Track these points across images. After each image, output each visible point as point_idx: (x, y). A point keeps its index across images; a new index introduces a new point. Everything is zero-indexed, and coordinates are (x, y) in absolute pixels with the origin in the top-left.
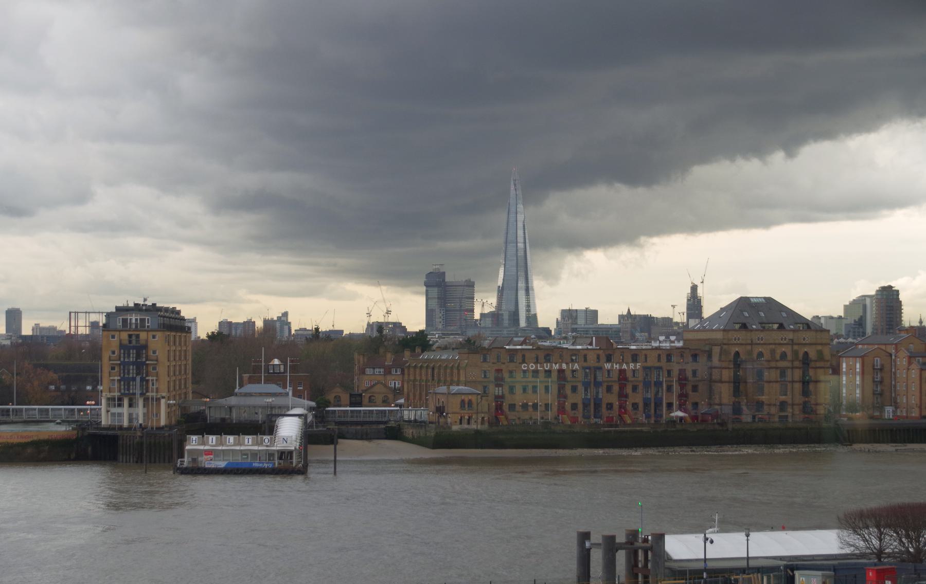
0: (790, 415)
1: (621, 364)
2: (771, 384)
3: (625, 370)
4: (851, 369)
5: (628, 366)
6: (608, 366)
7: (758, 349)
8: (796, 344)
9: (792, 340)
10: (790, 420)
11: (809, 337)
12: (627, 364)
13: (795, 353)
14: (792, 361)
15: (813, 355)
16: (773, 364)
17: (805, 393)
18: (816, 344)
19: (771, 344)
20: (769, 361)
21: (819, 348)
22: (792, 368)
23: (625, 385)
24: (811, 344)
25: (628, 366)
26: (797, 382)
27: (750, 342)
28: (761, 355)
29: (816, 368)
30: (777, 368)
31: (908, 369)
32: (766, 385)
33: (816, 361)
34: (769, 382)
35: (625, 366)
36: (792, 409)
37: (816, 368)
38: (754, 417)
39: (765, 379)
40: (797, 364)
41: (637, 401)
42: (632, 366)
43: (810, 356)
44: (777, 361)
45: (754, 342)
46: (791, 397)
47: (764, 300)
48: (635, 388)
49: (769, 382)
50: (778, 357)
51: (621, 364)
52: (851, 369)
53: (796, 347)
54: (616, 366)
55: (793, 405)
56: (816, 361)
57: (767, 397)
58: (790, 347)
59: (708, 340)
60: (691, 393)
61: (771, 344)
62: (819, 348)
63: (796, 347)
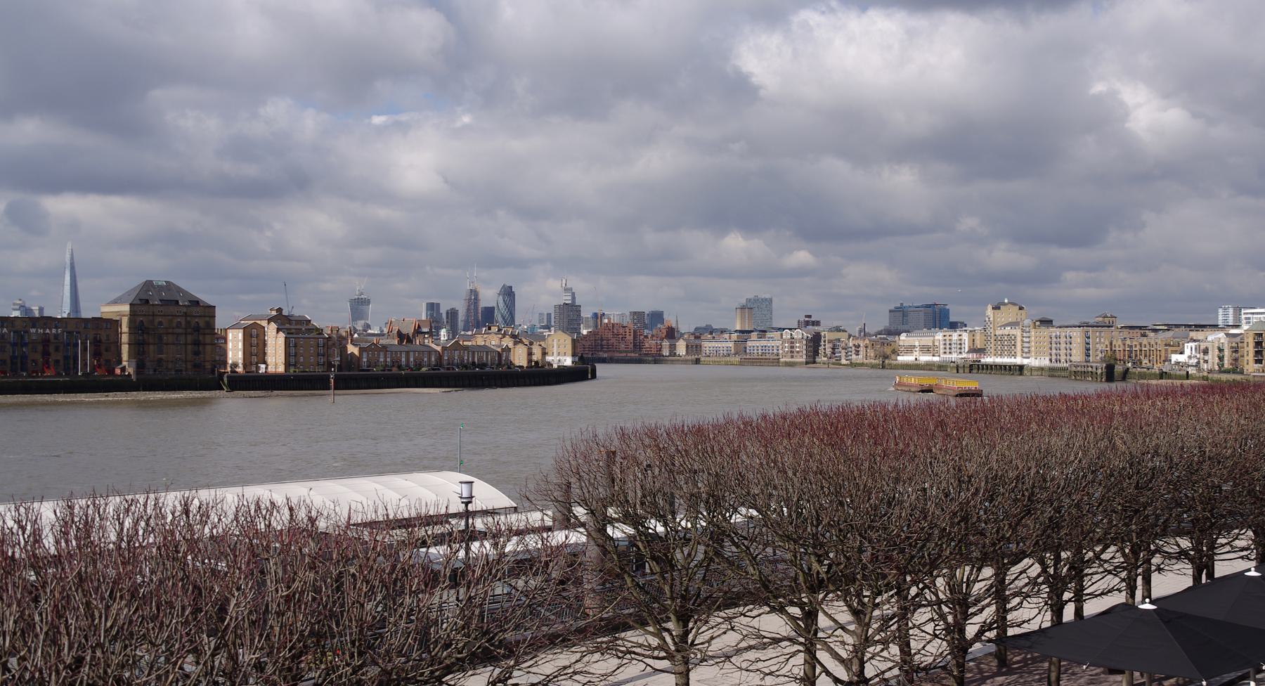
0: (184, 369)
1: (45, 329)
2: (169, 346)
3: (48, 333)
4: (235, 337)
5: (51, 331)
6: (33, 330)
7: (158, 319)
8: (189, 316)
9: (186, 313)
10: (184, 373)
11: (195, 310)
12: (50, 329)
13: (188, 323)
14: (186, 329)
15: (202, 324)
16: (170, 331)
17: (197, 353)
18: (205, 316)
19: (168, 316)
20: (166, 328)
21: (207, 319)
22: (186, 334)
23: (48, 346)
24: (200, 316)
25: (51, 331)
26: (189, 344)
27: (151, 313)
28: (160, 323)
29: (204, 334)
30: (173, 334)
31: (276, 337)
32: (165, 346)
33: (204, 329)
34: (167, 344)
35: (48, 331)
36: (186, 364)
37: (204, 334)
38: (155, 371)
39: (165, 341)
40: (189, 330)
41: (58, 358)
42: (54, 331)
43: (200, 325)
44: (173, 328)
45: (155, 313)
46: (184, 355)
47: (165, 284)
48: (57, 349)
49: (167, 344)
50: (174, 325)
51: (45, 329)
52: (235, 337)
53: (188, 318)
54: (41, 331)
55: (186, 361)
56: (204, 329)
57: (165, 356)
58: (184, 318)
59: (118, 312)
60: (104, 353)
61: (168, 316)
62: (207, 319)
63: (188, 318)
